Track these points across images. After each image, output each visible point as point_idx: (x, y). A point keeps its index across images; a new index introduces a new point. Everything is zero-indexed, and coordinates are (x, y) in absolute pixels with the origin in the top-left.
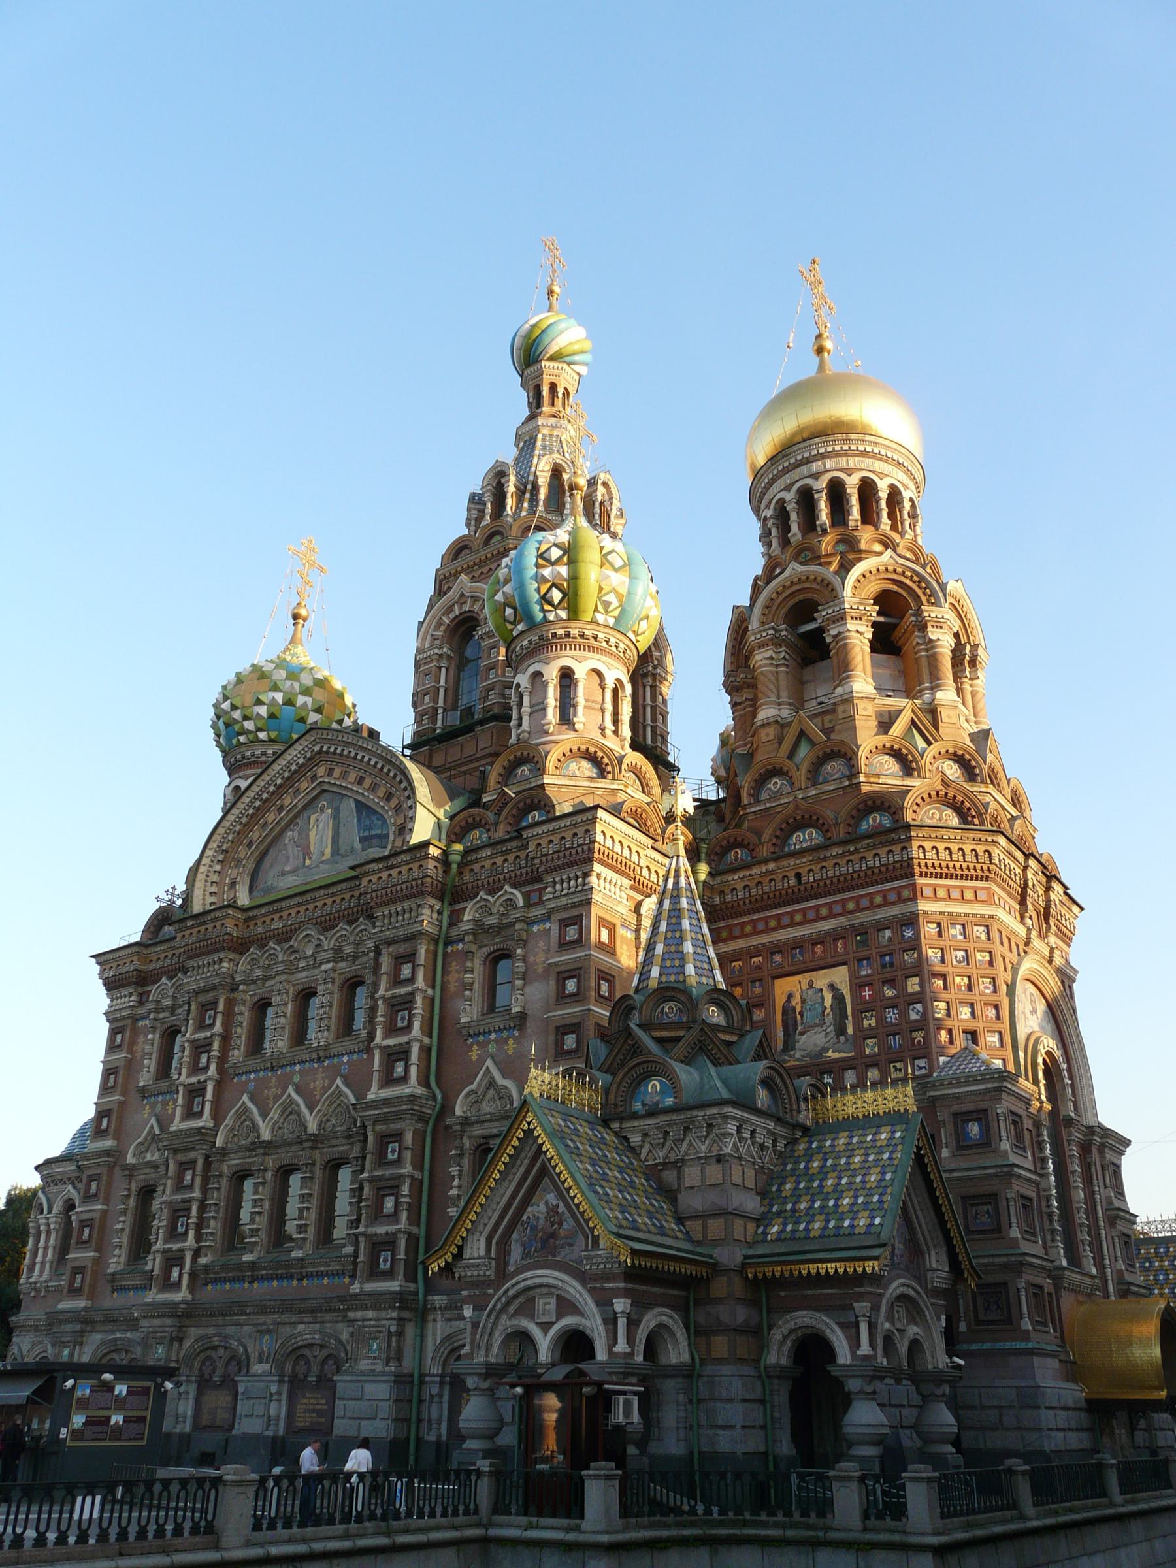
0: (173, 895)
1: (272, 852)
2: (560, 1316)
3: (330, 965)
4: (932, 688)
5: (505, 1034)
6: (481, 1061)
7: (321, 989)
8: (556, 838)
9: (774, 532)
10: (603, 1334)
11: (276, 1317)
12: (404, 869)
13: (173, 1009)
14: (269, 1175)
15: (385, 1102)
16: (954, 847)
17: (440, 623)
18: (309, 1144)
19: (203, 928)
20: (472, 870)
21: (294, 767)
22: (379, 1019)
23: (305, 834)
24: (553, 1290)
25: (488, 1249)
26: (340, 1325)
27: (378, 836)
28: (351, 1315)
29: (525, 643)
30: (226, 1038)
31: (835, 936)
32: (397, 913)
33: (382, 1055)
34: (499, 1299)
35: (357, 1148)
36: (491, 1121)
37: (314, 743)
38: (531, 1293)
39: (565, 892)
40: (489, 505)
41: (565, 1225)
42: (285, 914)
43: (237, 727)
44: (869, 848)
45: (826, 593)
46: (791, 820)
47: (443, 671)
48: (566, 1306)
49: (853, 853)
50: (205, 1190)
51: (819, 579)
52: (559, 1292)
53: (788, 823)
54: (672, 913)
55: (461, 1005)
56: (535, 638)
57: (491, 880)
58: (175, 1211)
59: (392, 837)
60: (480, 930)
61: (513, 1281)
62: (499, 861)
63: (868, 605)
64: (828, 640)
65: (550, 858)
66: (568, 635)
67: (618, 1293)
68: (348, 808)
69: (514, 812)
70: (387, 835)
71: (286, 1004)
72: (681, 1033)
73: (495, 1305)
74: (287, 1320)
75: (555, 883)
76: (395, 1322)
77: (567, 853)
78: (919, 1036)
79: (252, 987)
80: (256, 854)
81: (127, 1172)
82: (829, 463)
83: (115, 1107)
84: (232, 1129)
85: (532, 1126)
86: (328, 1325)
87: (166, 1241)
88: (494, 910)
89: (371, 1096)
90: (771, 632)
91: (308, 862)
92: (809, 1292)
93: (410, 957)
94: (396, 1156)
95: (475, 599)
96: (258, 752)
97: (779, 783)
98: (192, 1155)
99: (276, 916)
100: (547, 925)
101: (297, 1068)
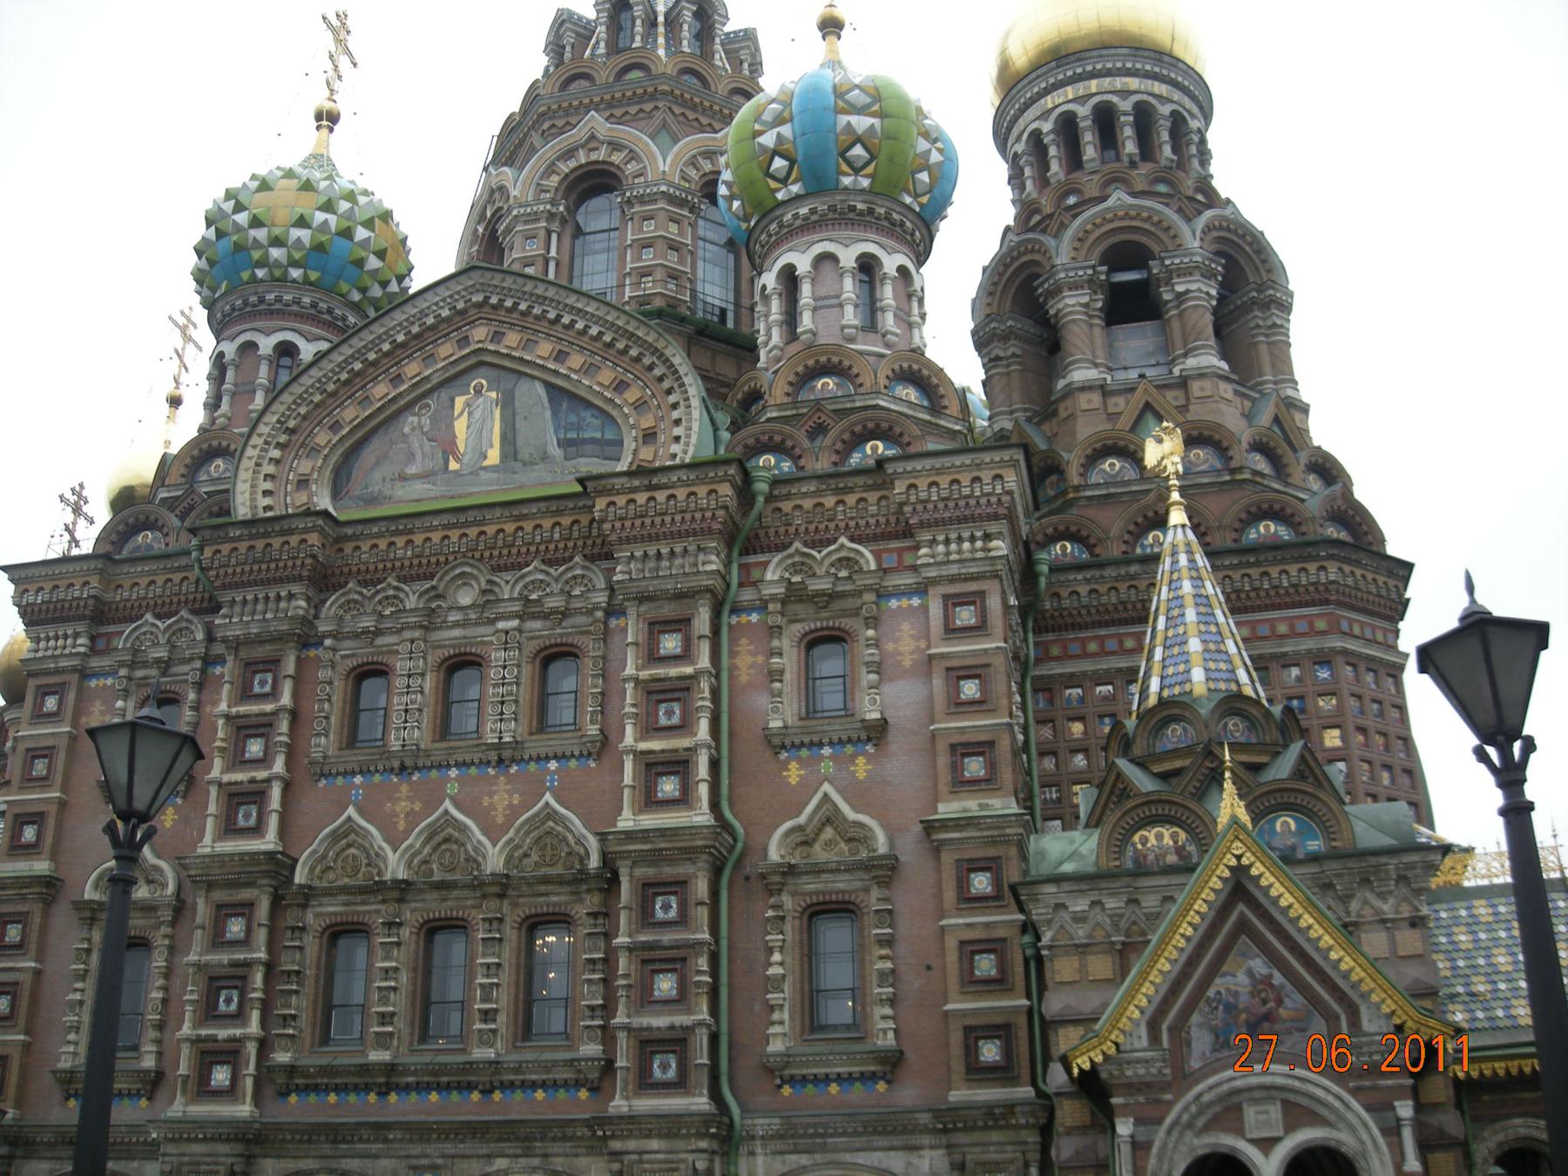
0: (80, 496)
2: (1290, 1128)
3: (515, 623)
4: (1275, 383)
5: (849, 749)
6: (808, 787)
7: (497, 656)
8: (944, 481)
9: (1053, 151)
10: (1385, 1149)
11: (449, 1148)
12: (681, 494)
13: (165, 666)
14: (405, 933)
15: (663, 833)
16: (1370, 576)
17: (551, 170)
18: (496, 889)
19: (260, 544)
20: (779, 510)
21: (430, 321)
22: (628, 709)
23: (445, 420)
24: (1274, 1093)
25: (1154, 1038)
26: (583, 1161)
27: (592, 441)
28: (616, 1145)
29: (804, 211)
30: (294, 715)
32: (659, 555)
33: (634, 761)
34: (1186, 1109)
35: (592, 901)
36: (832, 871)
37: (473, 289)
38: (1235, 1099)
39: (954, 557)
40: (603, 28)
41: (1287, 1002)
42: (418, 539)
43: (256, 255)
44: (1275, 562)
45: (1164, 237)
46: (1150, 514)
47: (554, 237)
48: (1297, 1112)
49: (1249, 565)
50: (271, 945)
51: (1156, 219)
52: (1285, 1095)
53: (1145, 517)
54: (1199, 600)
55: (761, 701)
56: (822, 208)
57: (812, 527)
58: (211, 978)
59: (629, 445)
60: (794, 595)
61: (1212, 1080)
62: (829, 501)
63: (1218, 264)
64: (1166, 297)
65: (930, 506)
66: (871, 211)
67: (1399, 1093)
68: (532, 394)
69: (846, 436)
70: (620, 443)
71: (423, 675)
72: (1264, 759)
73: (1179, 1117)
74: (468, 1152)
75: (933, 542)
76: (705, 1156)
77: (962, 503)
79: (347, 644)
80: (348, 444)
81: (88, 914)
82: (1133, 83)
83: (53, 810)
84: (324, 857)
85: (1245, 861)
86: (559, 1160)
87: (197, 1024)
88: (821, 571)
90: (1090, 272)
91: (453, 465)
92: (1526, 1095)
93: (681, 624)
94: (673, 914)
95: (615, 146)
96: (288, 297)
97: (1118, 465)
98: (245, 894)
99: (400, 541)
100: (916, 602)
101: (453, 773)
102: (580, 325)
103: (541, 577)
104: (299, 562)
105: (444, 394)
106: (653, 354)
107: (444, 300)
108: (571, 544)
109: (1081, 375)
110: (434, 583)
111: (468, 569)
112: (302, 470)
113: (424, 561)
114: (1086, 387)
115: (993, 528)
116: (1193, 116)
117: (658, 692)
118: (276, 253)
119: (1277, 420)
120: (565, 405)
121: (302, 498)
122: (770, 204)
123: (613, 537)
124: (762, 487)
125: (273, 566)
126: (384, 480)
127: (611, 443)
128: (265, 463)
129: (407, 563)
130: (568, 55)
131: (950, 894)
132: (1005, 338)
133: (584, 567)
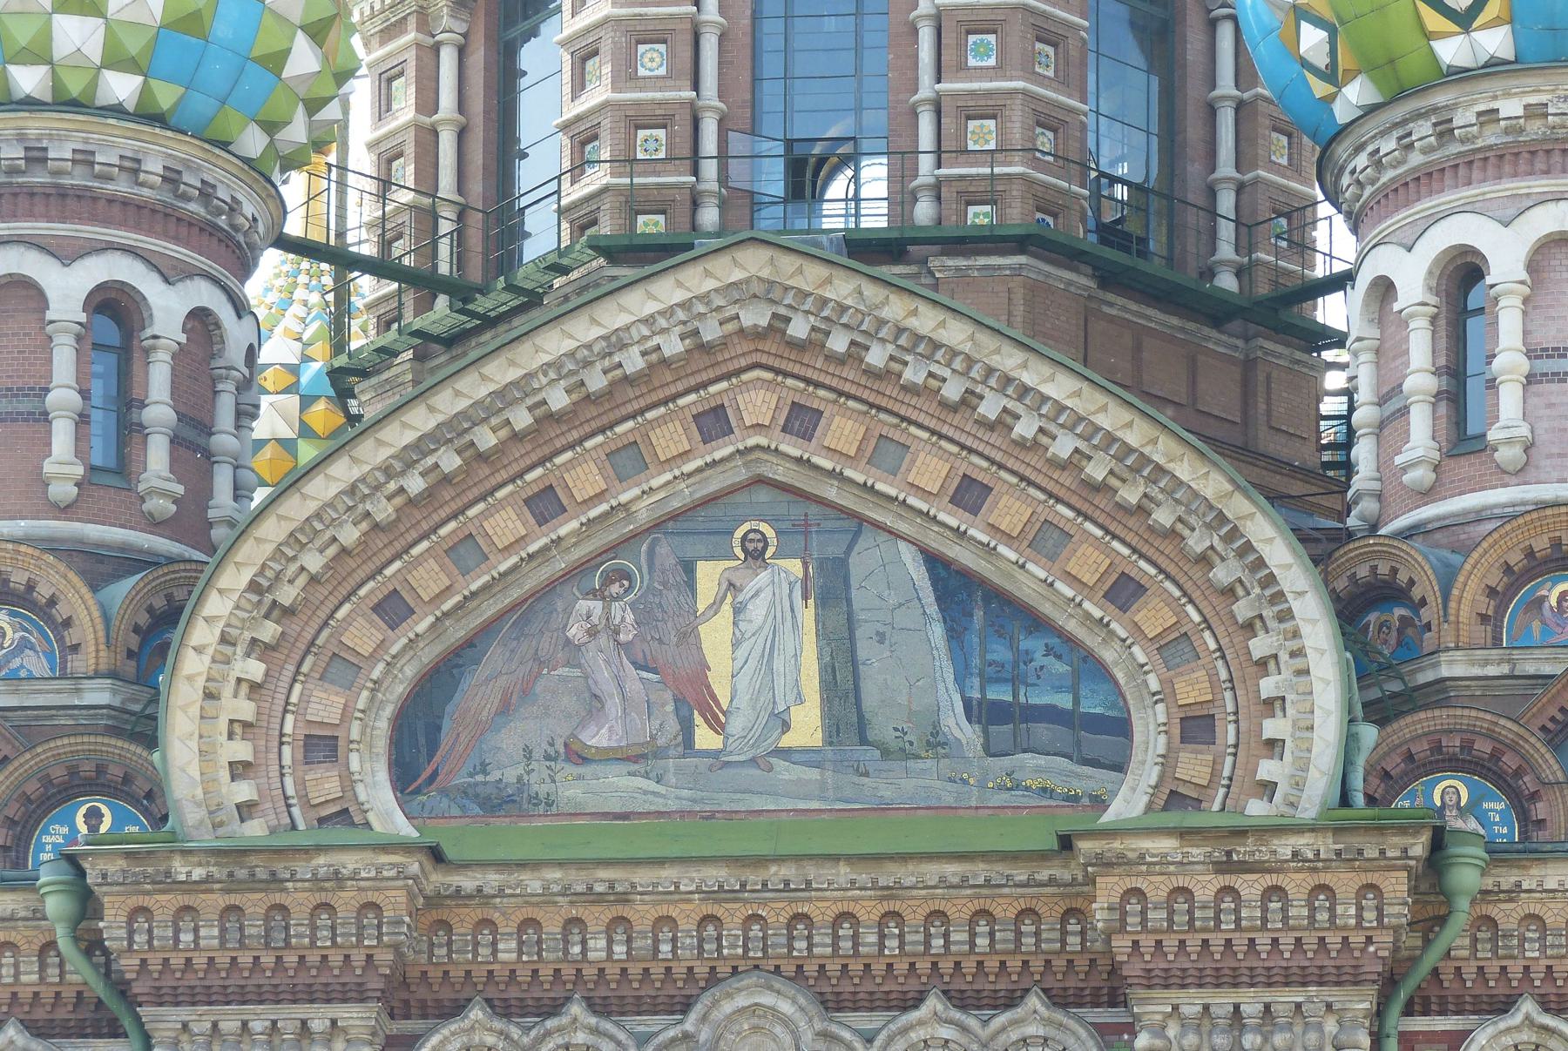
1: (495, 657)
19: (255, 903)
20: (1491, 922)
21: (633, 361)
27: (1051, 714)
70: (1121, 727)
80: (428, 654)
91: (705, 738)
99: (597, 917)
102: (1025, 428)
103: (946, 1032)
104: (358, 957)
105: (666, 552)
106: (1208, 526)
107: (669, 312)
108: (1014, 964)
110: (689, 1026)
111: (767, 999)
112: (316, 712)
113: (657, 970)
120: (979, 614)
121: (325, 784)
122: (1413, 67)
123: (1133, 970)
124: (1466, 877)
125: (291, 959)
126: (528, 754)
127: (1096, 724)
128: (227, 690)
129: (612, 971)
133: (1048, 1022)
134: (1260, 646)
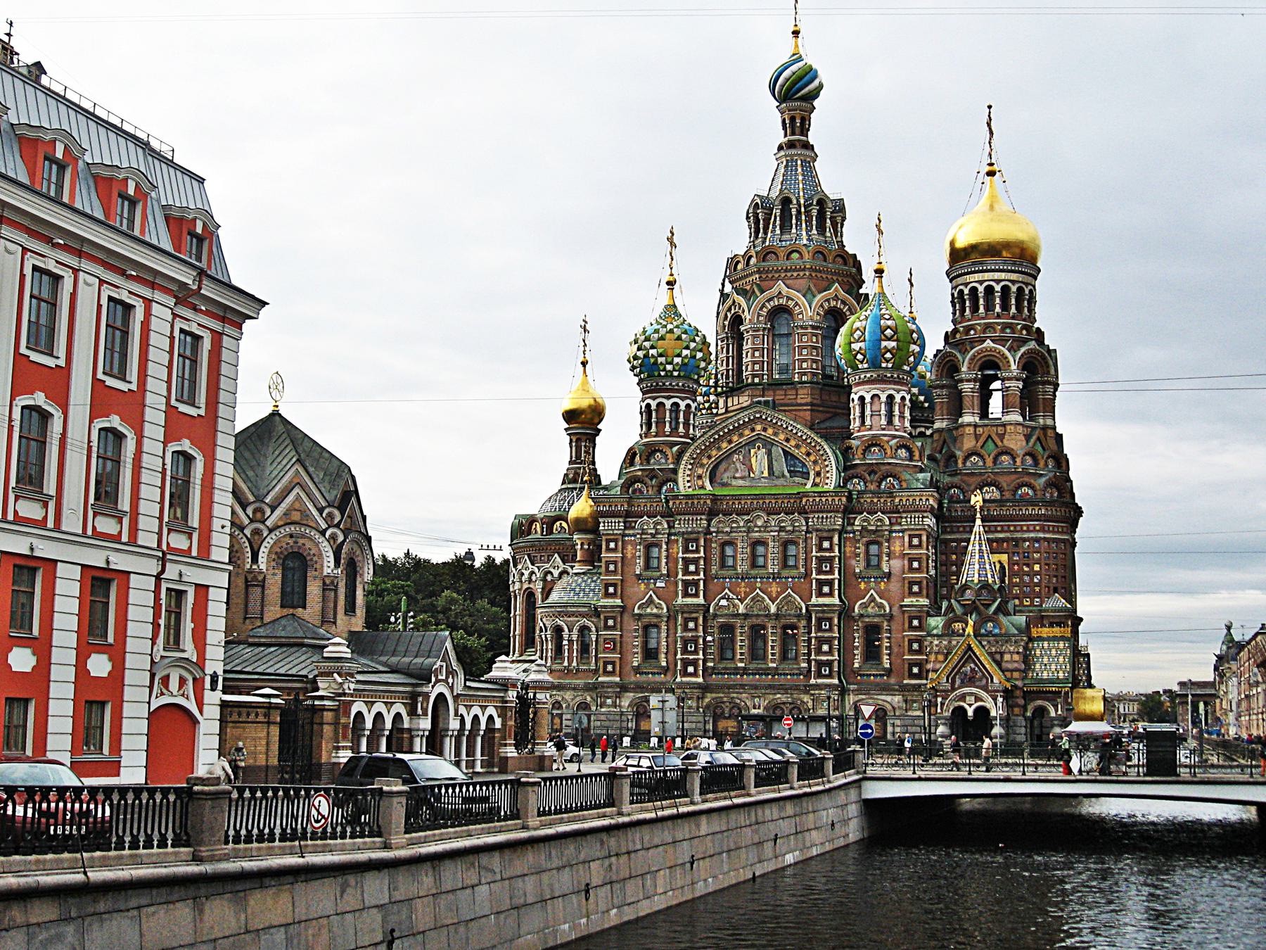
7: (771, 544)
9: (968, 303)
12: (830, 499)
19: (690, 502)
30: (705, 559)
31: (1003, 540)
48: (978, 699)
55: (853, 562)
68: (777, 452)
78: (1037, 589)
89: (814, 600)
91: (752, 475)
93: (830, 539)
95: (789, 298)
98: (694, 615)
99: (737, 502)
109: (967, 419)
114: (969, 425)
115: (925, 515)
116: (1027, 284)
117: (821, 560)
118: (669, 367)
119: (1038, 439)
121: (700, 483)
130: (761, 226)
131: (907, 625)
132: (943, 387)
134: (826, 463)
